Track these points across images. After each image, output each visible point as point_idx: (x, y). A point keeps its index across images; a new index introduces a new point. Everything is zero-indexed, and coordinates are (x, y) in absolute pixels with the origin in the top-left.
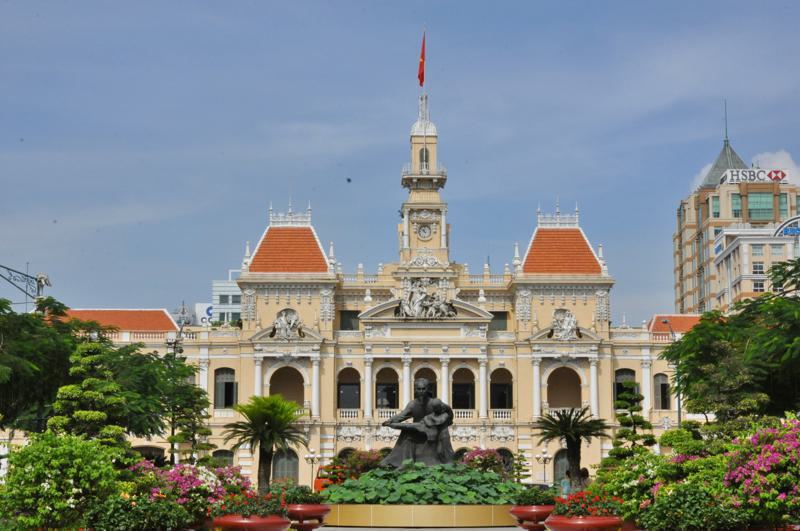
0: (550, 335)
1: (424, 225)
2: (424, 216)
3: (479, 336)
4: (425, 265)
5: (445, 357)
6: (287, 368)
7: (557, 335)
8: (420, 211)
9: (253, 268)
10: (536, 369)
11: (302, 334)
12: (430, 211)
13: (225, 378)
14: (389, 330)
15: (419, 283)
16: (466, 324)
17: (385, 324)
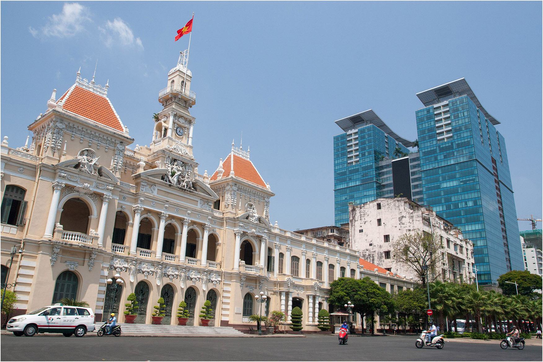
0: (247, 218)
1: (180, 127)
2: (182, 121)
3: (208, 209)
4: (180, 152)
5: (187, 218)
6: (78, 199)
7: (252, 219)
8: (181, 117)
9: (65, 106)
10: (238, 239)
11: (100, 174)
12: (186, 119)
13: (15, 196)
14: (156, 190)
15: (176, 163)
16: (203, 199)
17: (154, 184)
